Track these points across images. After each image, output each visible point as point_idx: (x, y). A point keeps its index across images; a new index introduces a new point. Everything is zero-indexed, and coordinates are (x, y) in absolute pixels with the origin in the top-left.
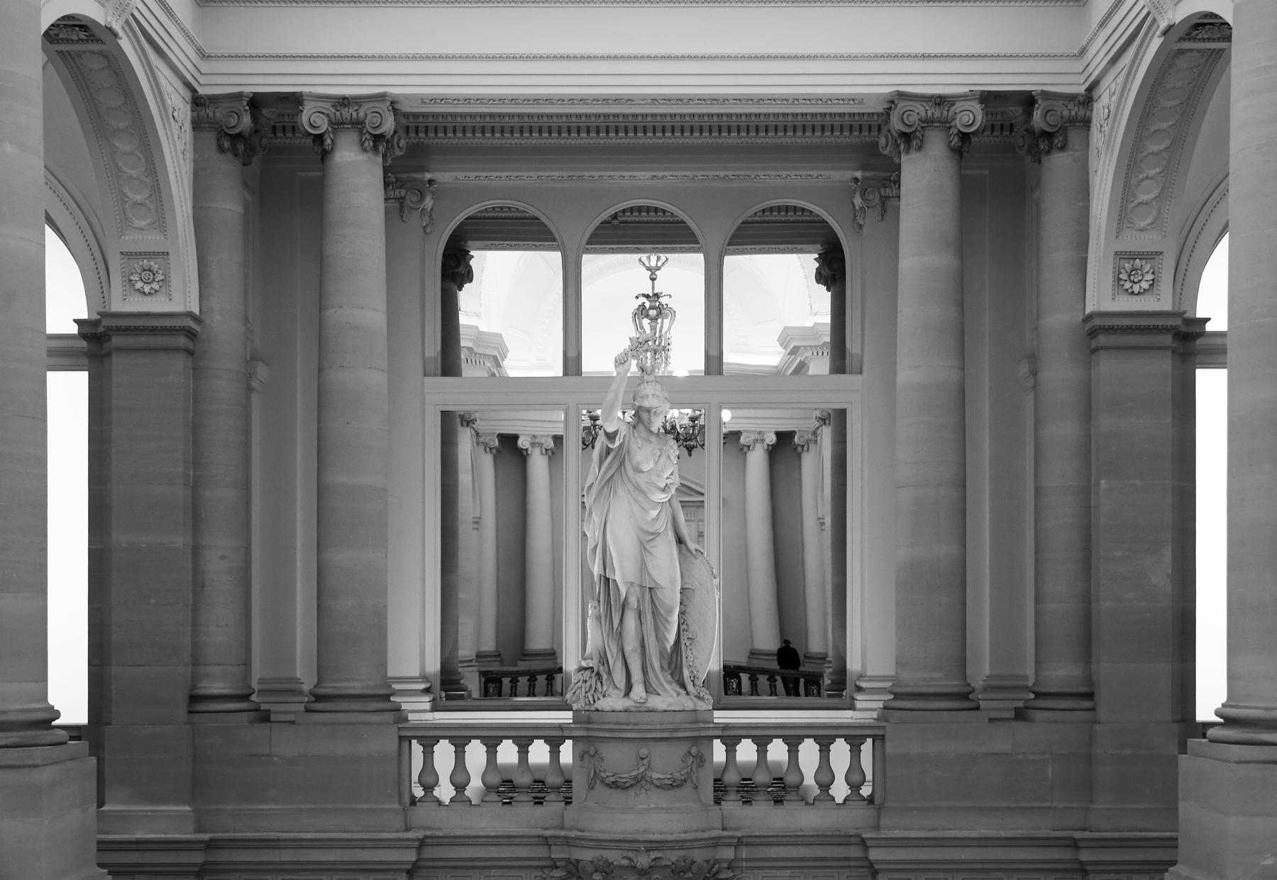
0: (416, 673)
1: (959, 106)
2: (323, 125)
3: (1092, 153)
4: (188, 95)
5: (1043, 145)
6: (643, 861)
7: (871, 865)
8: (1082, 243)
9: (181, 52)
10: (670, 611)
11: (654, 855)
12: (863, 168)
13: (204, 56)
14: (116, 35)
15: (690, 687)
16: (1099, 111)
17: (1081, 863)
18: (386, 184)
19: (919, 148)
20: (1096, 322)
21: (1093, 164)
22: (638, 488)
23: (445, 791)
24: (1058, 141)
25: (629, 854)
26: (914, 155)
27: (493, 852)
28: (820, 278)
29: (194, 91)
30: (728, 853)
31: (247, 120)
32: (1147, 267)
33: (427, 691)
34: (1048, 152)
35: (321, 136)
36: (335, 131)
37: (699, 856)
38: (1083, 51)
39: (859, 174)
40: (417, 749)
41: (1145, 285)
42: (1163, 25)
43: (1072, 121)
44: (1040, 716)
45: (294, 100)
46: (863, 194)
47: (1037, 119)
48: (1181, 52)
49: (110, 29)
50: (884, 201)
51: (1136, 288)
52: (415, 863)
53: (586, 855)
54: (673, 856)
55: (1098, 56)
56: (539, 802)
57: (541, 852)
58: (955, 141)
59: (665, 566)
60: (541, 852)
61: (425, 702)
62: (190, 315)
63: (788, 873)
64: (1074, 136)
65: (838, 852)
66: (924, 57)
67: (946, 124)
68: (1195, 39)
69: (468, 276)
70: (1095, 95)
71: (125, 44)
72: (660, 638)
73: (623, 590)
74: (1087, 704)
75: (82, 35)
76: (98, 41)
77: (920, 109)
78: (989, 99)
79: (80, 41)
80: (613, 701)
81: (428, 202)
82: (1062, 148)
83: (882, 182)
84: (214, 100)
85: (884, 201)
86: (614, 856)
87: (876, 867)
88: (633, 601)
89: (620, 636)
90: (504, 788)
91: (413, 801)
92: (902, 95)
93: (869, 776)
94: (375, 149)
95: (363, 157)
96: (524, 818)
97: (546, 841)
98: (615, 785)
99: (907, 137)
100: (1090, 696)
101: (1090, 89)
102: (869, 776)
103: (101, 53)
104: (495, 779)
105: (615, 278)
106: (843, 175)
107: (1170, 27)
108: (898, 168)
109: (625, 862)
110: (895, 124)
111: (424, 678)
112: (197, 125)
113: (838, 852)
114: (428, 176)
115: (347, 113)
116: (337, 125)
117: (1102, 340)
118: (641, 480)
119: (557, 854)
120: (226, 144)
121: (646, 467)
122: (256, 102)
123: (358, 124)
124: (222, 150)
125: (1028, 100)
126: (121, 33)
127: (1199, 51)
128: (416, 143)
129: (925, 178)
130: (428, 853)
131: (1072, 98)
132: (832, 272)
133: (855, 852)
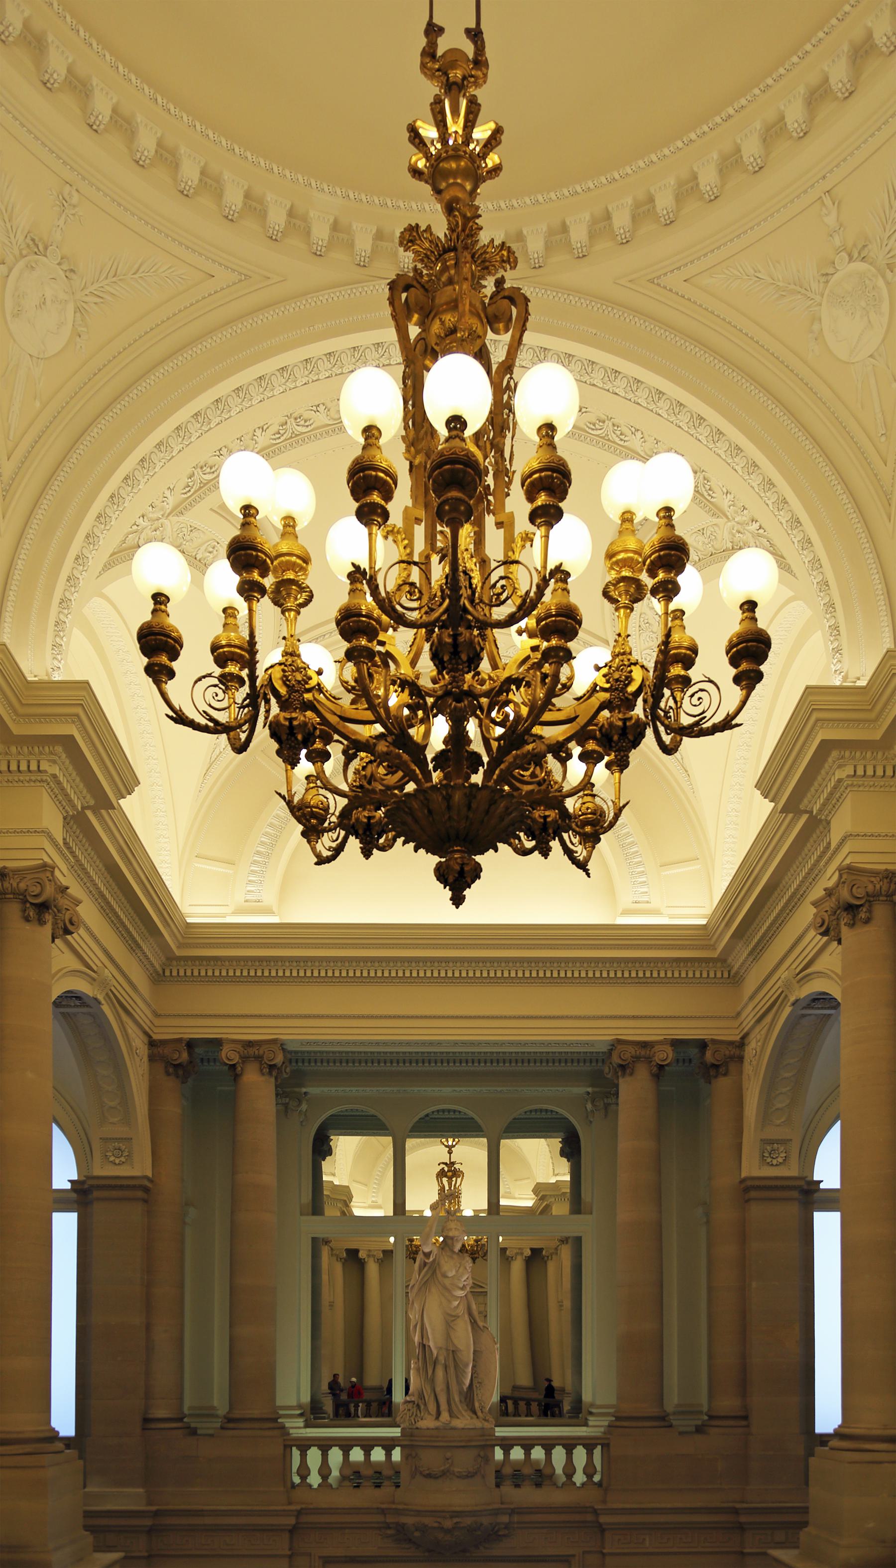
0: (294, 1403)
1: (657, 1048)
2: (235, 1059)
3: (745, 1077)
4: (146, 1040)
5: (712, 1072)
6: (448, 1524)
9: (142, 1012)
11: (455, 1520)
12: (592, 1086)
13: (157, 1015)
14: (100, 1003)
18: (277, 1095)
19: (631, 1074)
21: (745, 1084)
23: (315, 1480)
24: (722, 1070)
26: (628, 1078)
28: (563, 1153)
29: (150, 1037)
31: (185, 1055)
32: (782, 1149)
33: (301, 1415)
34: (716, 1077)
35: (233, 1067)
36: (243, 1062)
37: (486, 1521)
38: (739, 1014)
39: (590, 1090)
40: (296, 1453)
41: (780, 1160)
42: (792, 999)
43: (732, 1058)
45: (217, 1043)
46: (593, 1102)
47: (709, 1056)
48: (804, 1016)
49: (96, 999)
50: (607, 1106)
51: (775, 1162)
53: (409, 1520)
54: (468, 1521)
56: (378, 1486)
57: (380, 1518)
58: (655, 1069)
60: (380, 1518)
61: (300, 1422)
64: (732, 1067)
66: (634, 1017)
67: (649, 1060)
68: (813, 1008)
69: (329, 1152)
70: (746, 1041)
71: (106, 1008)
75: (78, 1003)
76: (88, 1006)
77: (632, 1051)
78: (676, 1044)
79: (76, 1006)
81: (304, 1107)
82: (725, 1075)
83: (605, 1093)
84: (164, 1042)
85: (607, 1106)
86: (427, 1521)
90: (354, 1476)
91: (293, 1486)
92: (619, 1041)
94: (270, 1073)
95: (262, 1078)
96: (367, 1497)
97: (383, 1512)
99: (623, 1067)
101: (743, 1038)
103: (89, 1014)
104: (348, 1472)
105: (426, 1155)
106: (580, 1090)
107: (797, 1001)
108: (617, 1086)
110: (616, 1060)
111: (300, 1406)
112: (152, 1059)
114: (304, 1090)
115: (252, 1051)
116: (245, 1059)
119: (390, 1519)
120: (171, 1070)
122: (191, 1044)
123: (259, 1058)
124: (168, 1074)
125: (703, 1045)
126: (103, 1002)
127: (816, 1015)
128: (294, 1070)
131: (731, 1043)
132: (571, 1150)
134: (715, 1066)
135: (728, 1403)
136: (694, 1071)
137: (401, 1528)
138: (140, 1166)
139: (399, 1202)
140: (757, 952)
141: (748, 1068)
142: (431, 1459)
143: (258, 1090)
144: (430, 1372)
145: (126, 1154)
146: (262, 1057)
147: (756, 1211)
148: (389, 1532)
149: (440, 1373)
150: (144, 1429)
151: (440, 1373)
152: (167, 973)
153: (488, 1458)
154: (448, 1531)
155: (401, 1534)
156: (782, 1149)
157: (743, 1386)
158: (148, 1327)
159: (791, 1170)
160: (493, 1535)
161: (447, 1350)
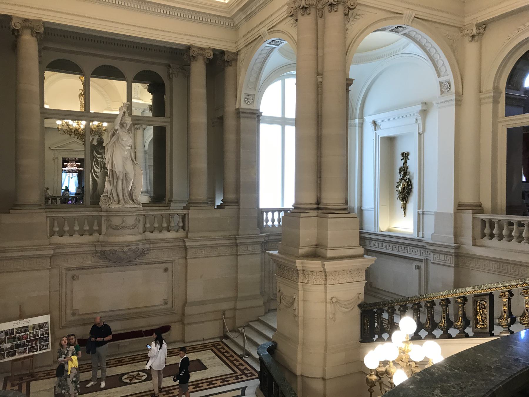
2: (19, 27)
11: (129, 247)
15: (135, 201)
17: (236, 243)
21: (238, 71)
25: (122, 248)
30: (147, 246)
44: (226, 207)
53: (108, 249)
54: (134, 248)
55: (241, 44)
56: (91, 235)
59: (129, 167)
65: (177, 244)
72: (128, 187)
73: (118, 174)
74: (237, 204)
80: (114, 206)
86: (116, 248)
89: (116, 187)
100: (237, 202)
109: (120, 250)
115: (27, 24)
116: (24, 27)
118: (123, 143)
119: (99, 249)
121: (125, 139)
123: (32, 29)
137: (103, 253)
140: (248, 18)
148: (98, 255)
154: (125, 253)
155: (104, 255)
160: (143, 253)
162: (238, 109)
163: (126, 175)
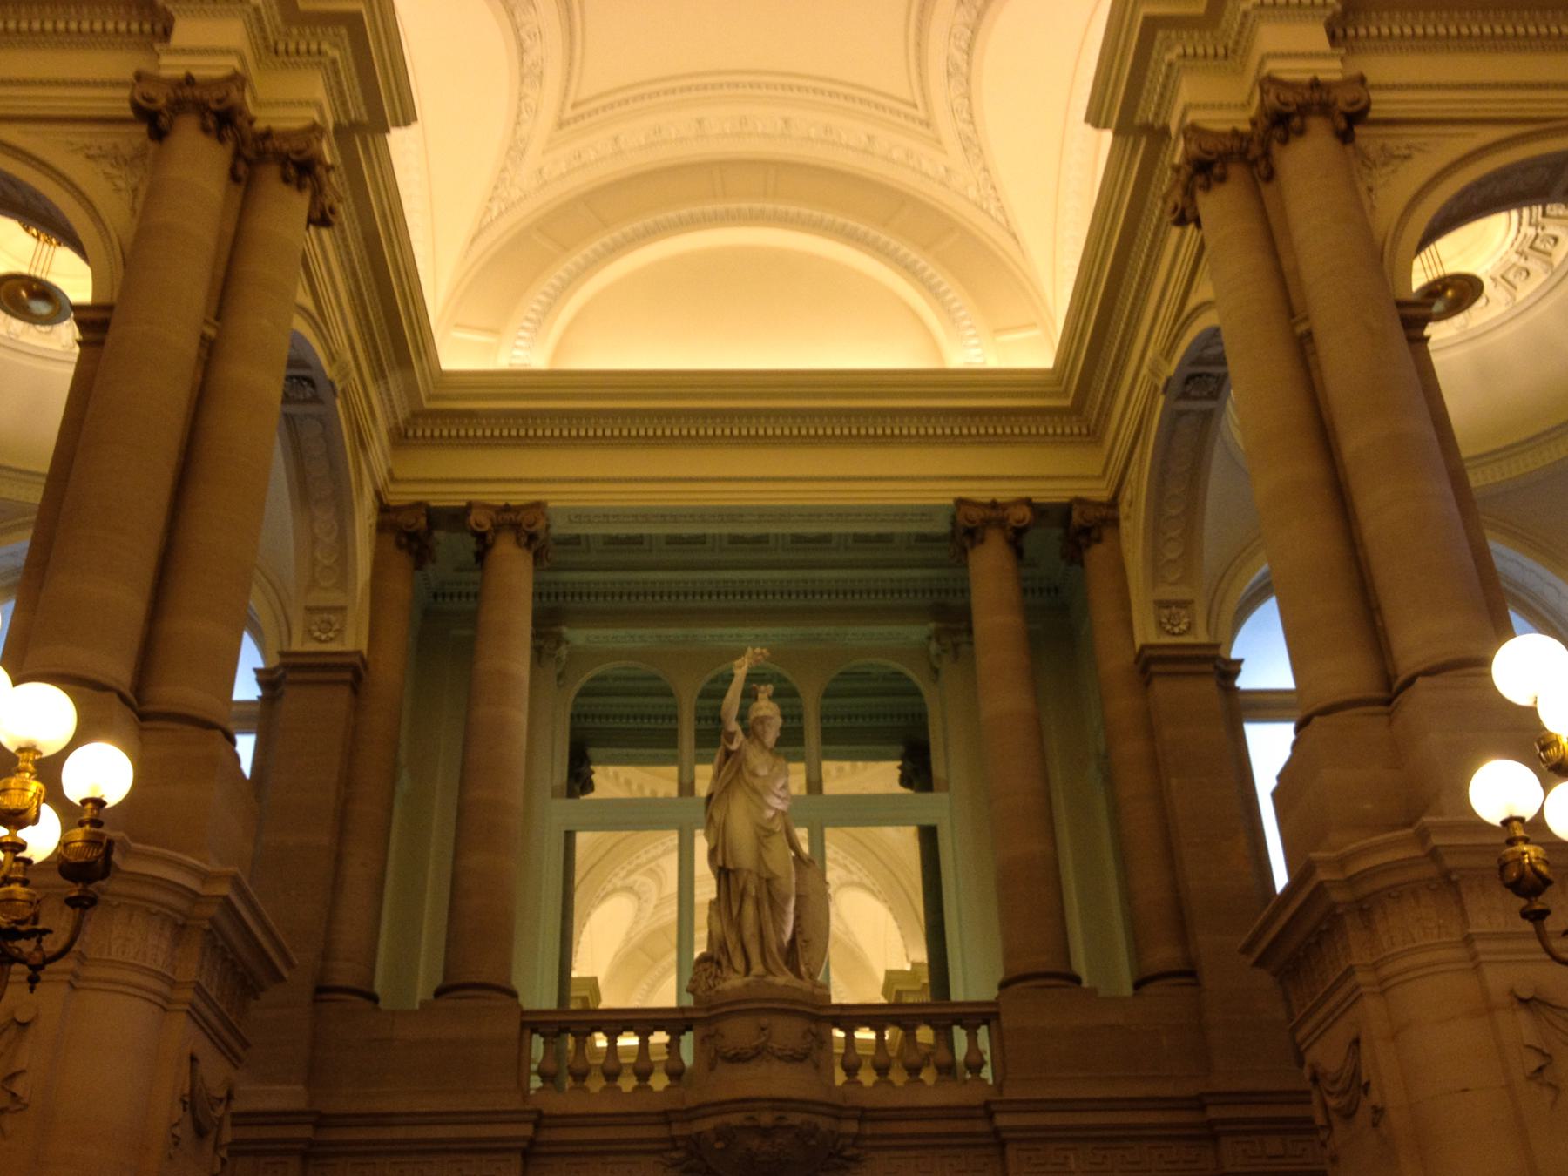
5: (1083, 540)
6: (766, 1119)
7: (996, 1132)
8: (1126, 605)
10: (786, 900)
14: (335, 393)
16: (1124, 509)
20: (1148, 652)
22: (755, 791)
24: (1094, 534)
27: (612, 1133)
30: (852, 1127)
31: (423, 521)
34: (1088, 546)
37: (824, 1123)
41: (1183, 627)
46: (938, 640)
48: (1181, 414)
50: (956, 646)
51: (1176, 630)
52: (532, 1142)
57: (662, 1132)
58: (1010, 534)
60: (662, 1132)
62: (358, 653)
63: (913, 1153)
67: (1001, 523)
72: (780, 931)
79: (305, 401)
83: (953, 619)
84: (399, 509)
86: (736, 1119)
87: (1004, 1135)
88: (752, 890)
89: (737, 924)
93: (987, 1057)
94: (528, 546)
98: (738, 1058)
102: (987, 1057)
106: (916, 632)
113: (962, 1126)
115: (507, 516)
116: (497, 528)
117: (1154, 668)
118: (757, 783)
119: (677, 1130)
120: (404, 540)
121: (763, 772)
123: (515, 527)
124: (399, 545)
129: (990, 575)
130: (546, 1135)
131: (1101, 504)
133: (981, 1126)
134: (1086, 531)
135: (1164, 955)
136: (1060, 545)
138: (353, 639)
139: (686, 780)
141: (1125, 526)
142: (739, 1033)
143: (515, 572)
144: (735, 911)
145: (337, 627)
146: (519, 525)
147: (1164, 690)
149: (749, 909)
150: (315, 1001)
151: (749, 909)
152: (410, 433)
153: (825, 1041)
154: (766, 1132)
156: (1183, 612)
157: (1181, 926)
158: (339, 858)
159: (1202, 637)
161: (760, 878)
162: (1144, 647)
163: (768, 882)
